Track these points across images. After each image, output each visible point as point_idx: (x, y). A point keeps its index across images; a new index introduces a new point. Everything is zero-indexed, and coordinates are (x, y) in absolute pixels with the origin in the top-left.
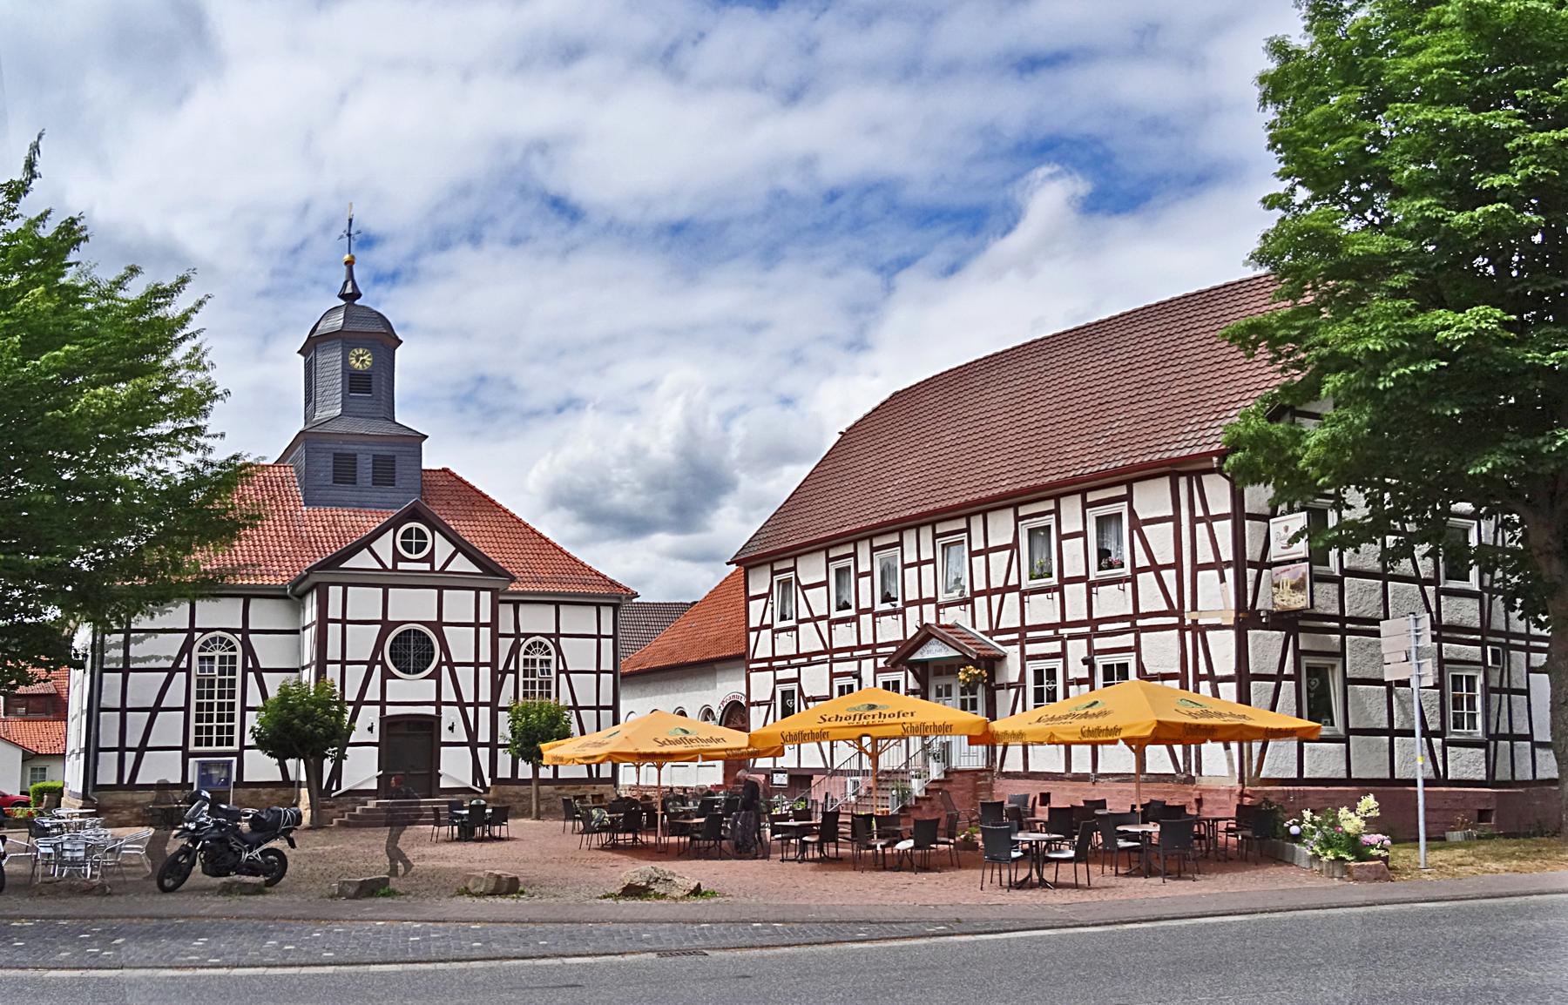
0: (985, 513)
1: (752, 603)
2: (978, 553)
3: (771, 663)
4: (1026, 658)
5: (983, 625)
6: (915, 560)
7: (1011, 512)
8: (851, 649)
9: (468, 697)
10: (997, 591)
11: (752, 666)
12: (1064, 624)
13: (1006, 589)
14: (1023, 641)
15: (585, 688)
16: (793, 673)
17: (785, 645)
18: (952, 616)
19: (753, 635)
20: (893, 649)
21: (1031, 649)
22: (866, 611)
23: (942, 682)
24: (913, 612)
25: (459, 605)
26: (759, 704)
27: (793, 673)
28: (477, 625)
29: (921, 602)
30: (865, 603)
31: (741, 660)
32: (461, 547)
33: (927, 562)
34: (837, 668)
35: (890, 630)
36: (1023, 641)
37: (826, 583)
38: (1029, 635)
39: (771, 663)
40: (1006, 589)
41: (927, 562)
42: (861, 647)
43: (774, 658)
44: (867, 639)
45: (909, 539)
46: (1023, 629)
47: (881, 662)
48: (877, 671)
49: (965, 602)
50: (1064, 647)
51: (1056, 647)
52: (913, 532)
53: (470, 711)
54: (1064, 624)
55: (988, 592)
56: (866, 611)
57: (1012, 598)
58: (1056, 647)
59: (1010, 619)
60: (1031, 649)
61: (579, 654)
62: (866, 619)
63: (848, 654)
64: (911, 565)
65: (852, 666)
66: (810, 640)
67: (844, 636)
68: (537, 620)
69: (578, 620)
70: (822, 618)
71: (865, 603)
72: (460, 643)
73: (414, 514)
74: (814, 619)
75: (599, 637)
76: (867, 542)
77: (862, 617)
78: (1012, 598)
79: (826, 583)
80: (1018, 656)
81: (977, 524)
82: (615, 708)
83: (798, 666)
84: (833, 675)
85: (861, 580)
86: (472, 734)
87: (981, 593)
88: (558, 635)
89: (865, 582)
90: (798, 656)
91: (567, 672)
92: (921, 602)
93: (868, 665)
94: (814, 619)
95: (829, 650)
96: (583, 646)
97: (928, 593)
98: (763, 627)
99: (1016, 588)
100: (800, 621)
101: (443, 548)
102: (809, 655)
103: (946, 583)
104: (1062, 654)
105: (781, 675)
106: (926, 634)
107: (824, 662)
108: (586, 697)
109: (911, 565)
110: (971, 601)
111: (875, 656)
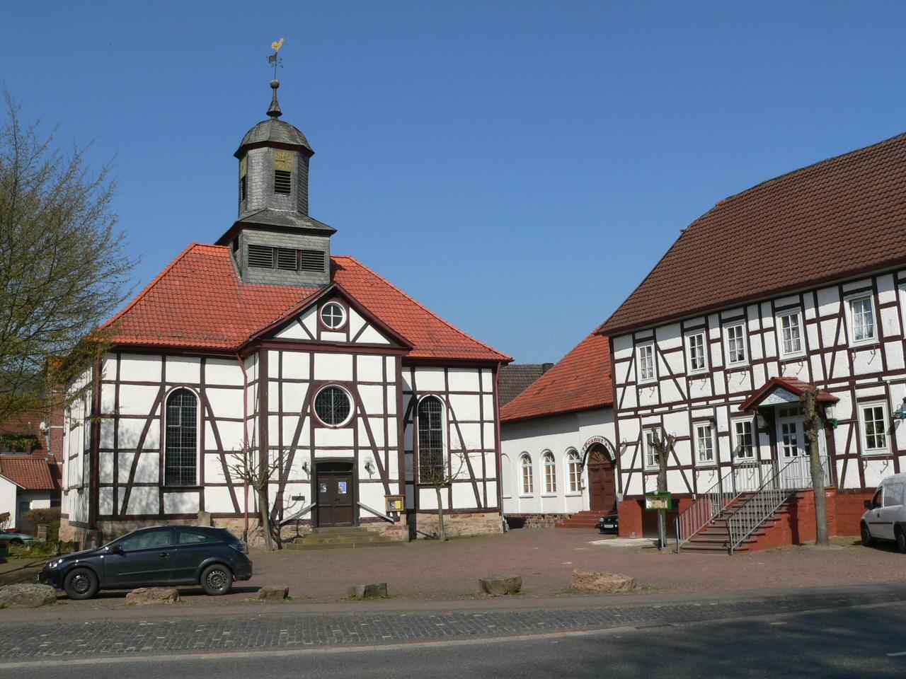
0: (815, 291)
1: (617, 365)
2: (811, 321)
3: (636, 412)
4: (856, 401)
5: (818, 376)
6: (758, 328)
7: (678, 326)
8: (707, 399)
9: (380, 443)
10: (829, 350)
11: (619, 415)
12: (886, 372)
13: (836, 348)
14: (852, 388)
15: (471, 436)
16: (657, 419)
17: (649, 397)
18: (791, 371)
19: (619, 391)
20: (744, 398)
21: (860, 393)
22: (718, 369)
23: (788, 421)
24: (758, 369)
25: (370, 367)
26: (628, 444)
27: (657, 419)
28: (385, 384)
29: (765, 360)
30: (717, 362)
31: (607, 410)
32: (371, 320)
33: (769, 330)
34: (696, 414)
35: (740, 383)
36: (852, 388)
37: (682, 348)
38: (858, 382)
39: (636, 412)
40: (836, 348)
41: (769, 330)
42: (715, 397)
43: (639, 408)
44: (720, 390)
45: (753, 310)
46: (852, 378)
47: (735, 408)
48: (731, 415)
49: (877, 346)
50: (887, 390)
51: (881, 390)
52: (755, 308)
53: (382, 454)
54: (886, 372)
55: (822, 351)
56: (718, 369)
57: (842, 356)
58: (881, 390)
59: (841, 370)
60: (860, 393)
61: (464, 407)
62: (719, 376)
63: (704, 403)
64: (755, 333)
65: (709, 412)
66: (670, 392)
67: (700, 389)
68: (428, 381)
69: (463, 380)
70: (680, 375)
71: (717, 362)
72: (371, 399)
73: (336, 293)
74: (673, 377)
75: (481, 393)
76: (716, 316)
77: (715, 374)
78: (842, 356)
79: (682, 348)
80: (850, 398)
81: (808, 298)
82: (497, 451)
83: (661, 414)
84: (692, 420)
85: (712, 345)
86: (384, 474)
87: (815, 352)
88: (447, 392)
89: (716, 347)
90: (661, 405)
91: (455, 422)
92: (765, 360)
93: (722, 412)
94: (673, 377)
95: (689, 401)
96: (468, 401)
97: (771, 352)
98: (628, 384)
99: (845, 347)
100: (660, 379)
101: (356, 321)
102: (670, 405)
103: (772, 348)
104: (887, 397)
105: (646, 421)
106: (774, 385)
107: (684, 410)
108: (472, 441)
109: (755, 333)
110: (807, 359)
111: (728, 404)
